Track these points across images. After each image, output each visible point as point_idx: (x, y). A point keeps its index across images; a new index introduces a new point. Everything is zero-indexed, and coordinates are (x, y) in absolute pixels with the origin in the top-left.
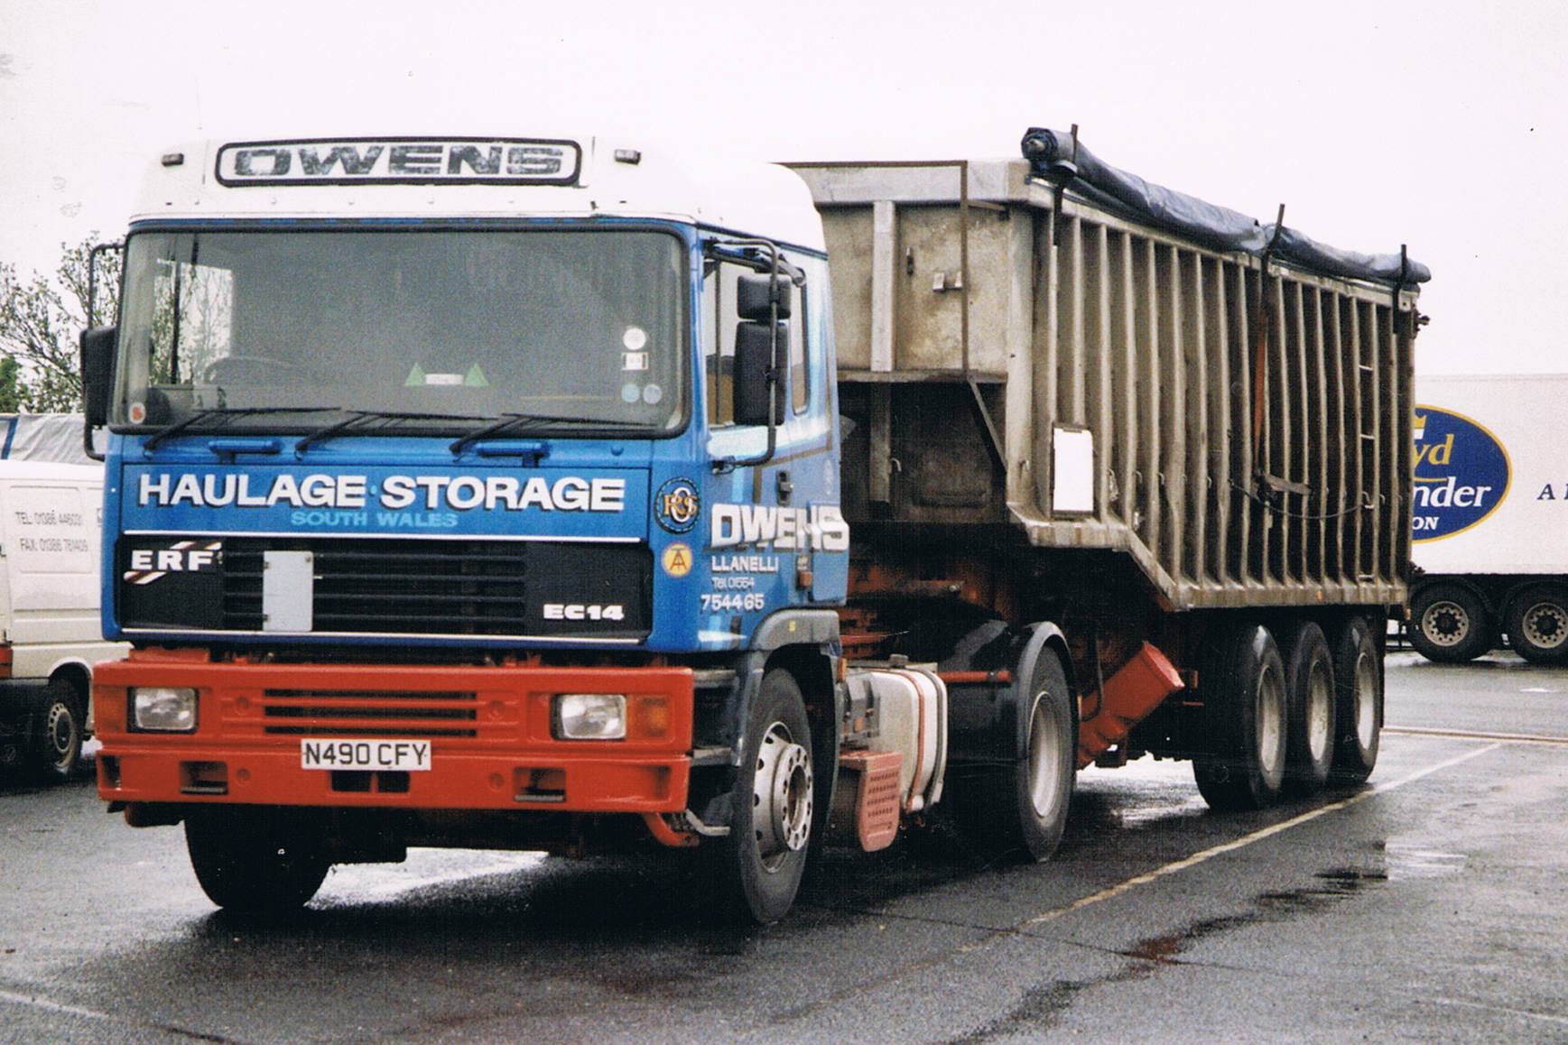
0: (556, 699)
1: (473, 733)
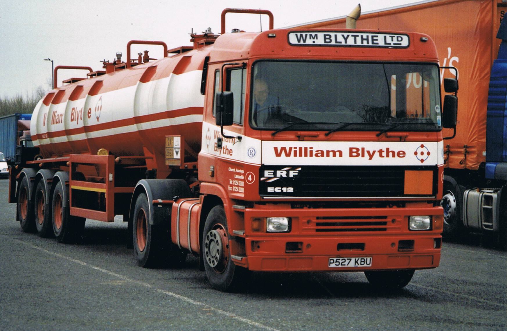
0: (408, 218)
1: (385, 229)
